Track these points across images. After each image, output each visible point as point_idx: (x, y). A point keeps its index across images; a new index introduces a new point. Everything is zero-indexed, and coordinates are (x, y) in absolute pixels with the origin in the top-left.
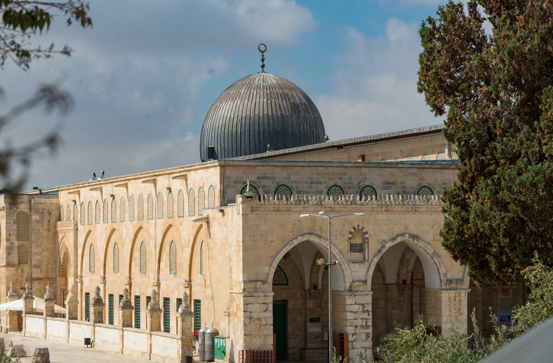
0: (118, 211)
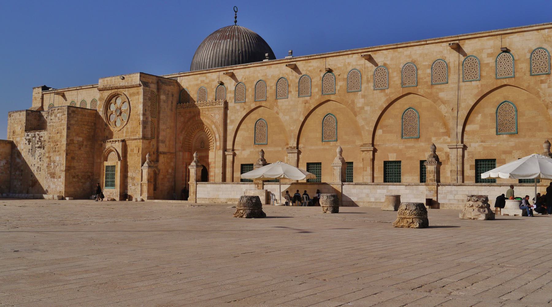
0: (341, 84)
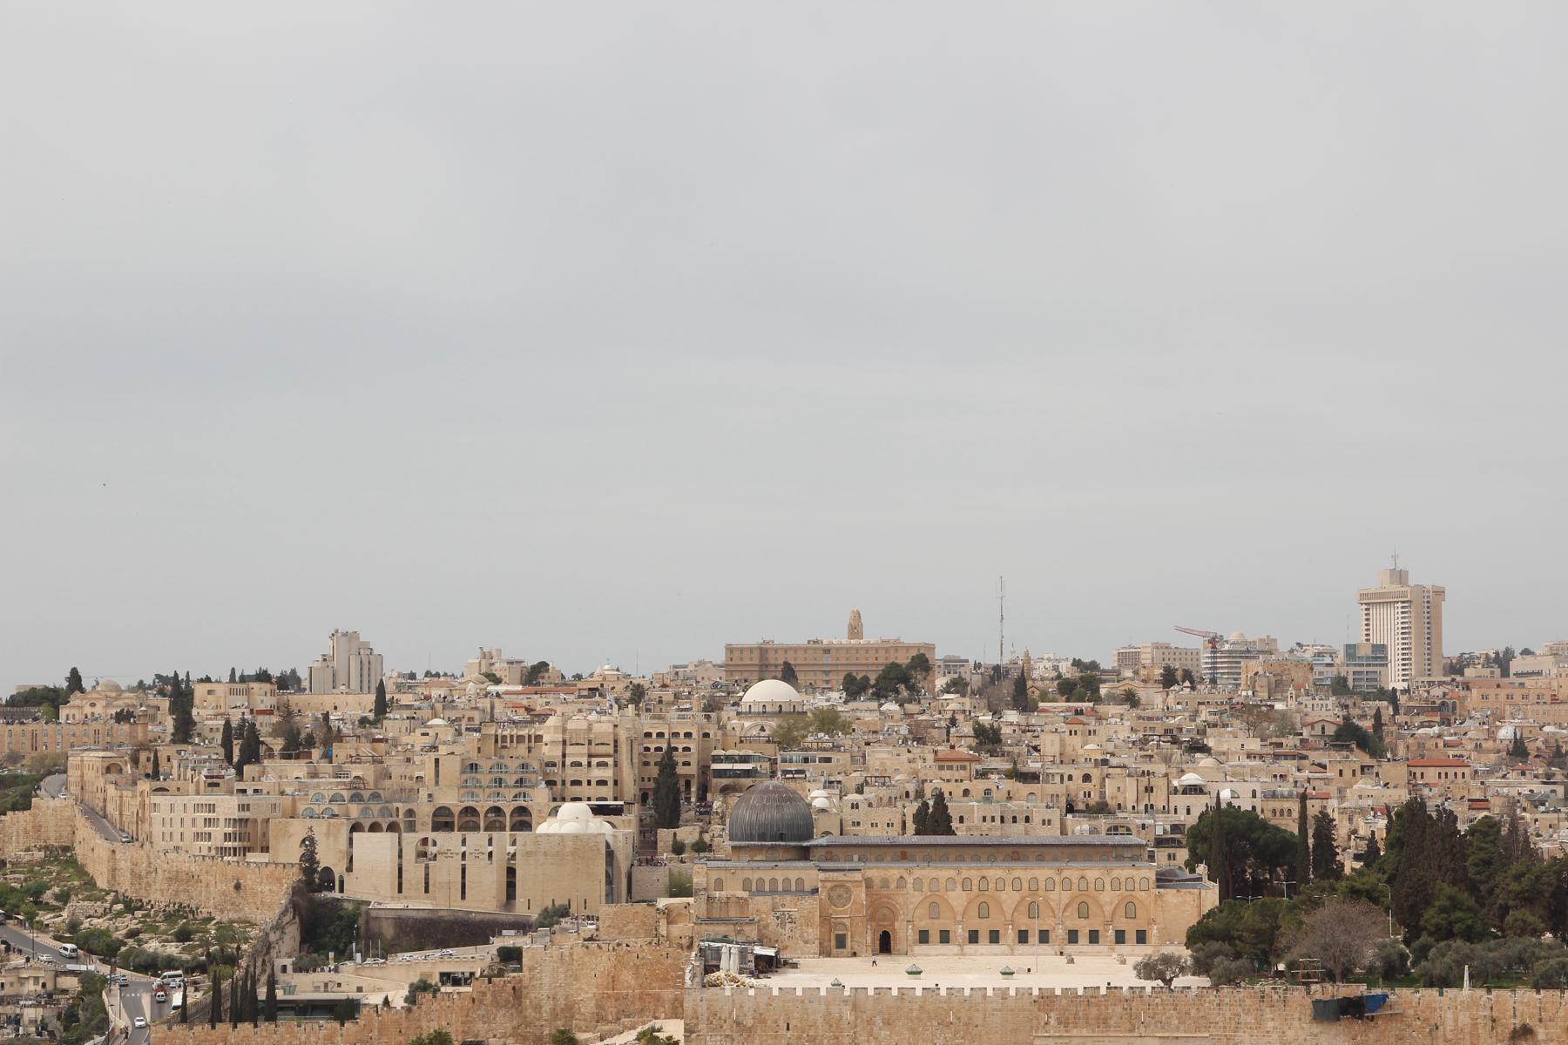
0: (992, 885)
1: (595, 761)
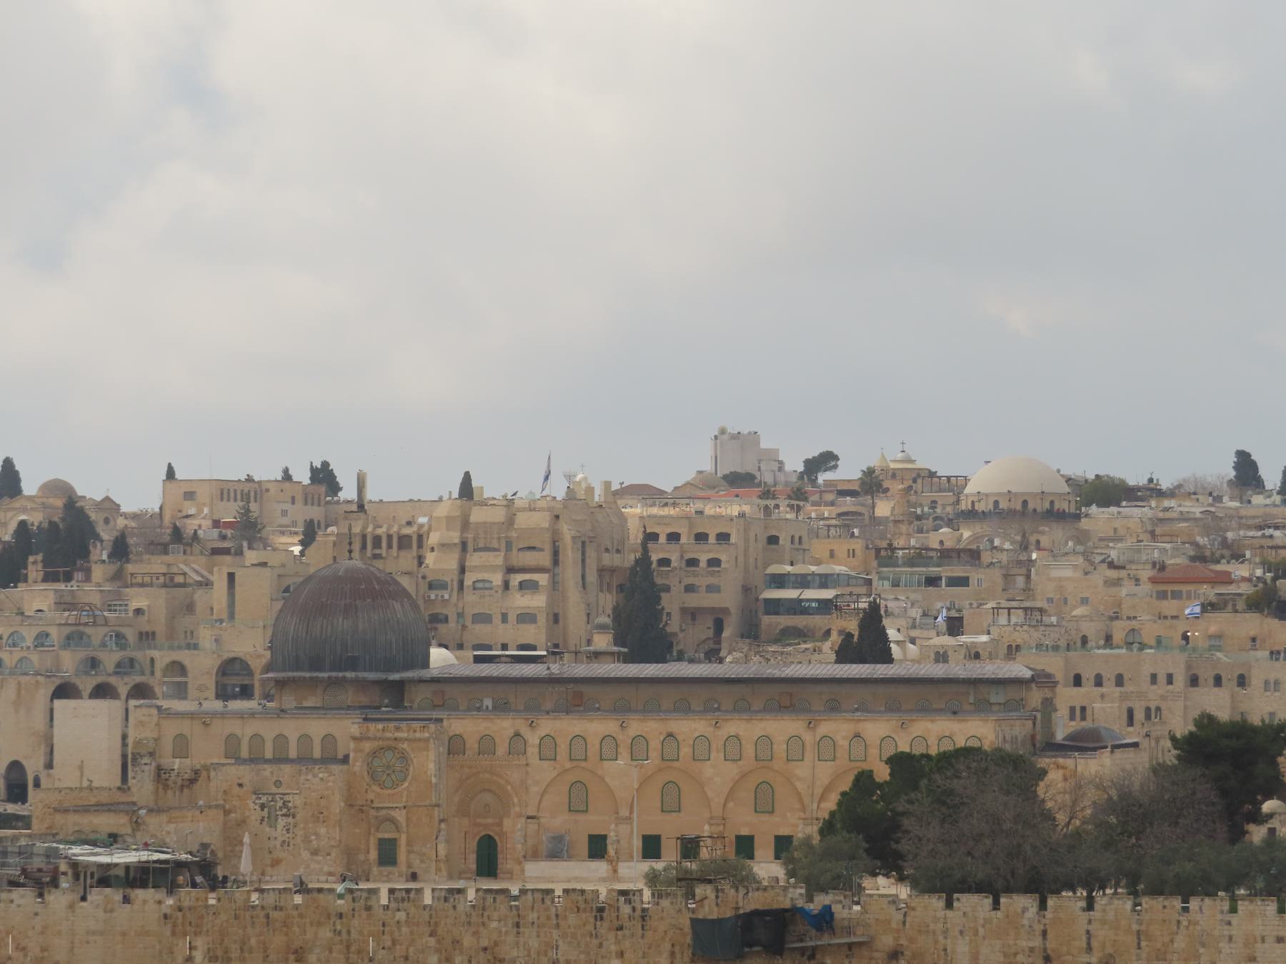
0: (686, 751)
1: (517, 579)
